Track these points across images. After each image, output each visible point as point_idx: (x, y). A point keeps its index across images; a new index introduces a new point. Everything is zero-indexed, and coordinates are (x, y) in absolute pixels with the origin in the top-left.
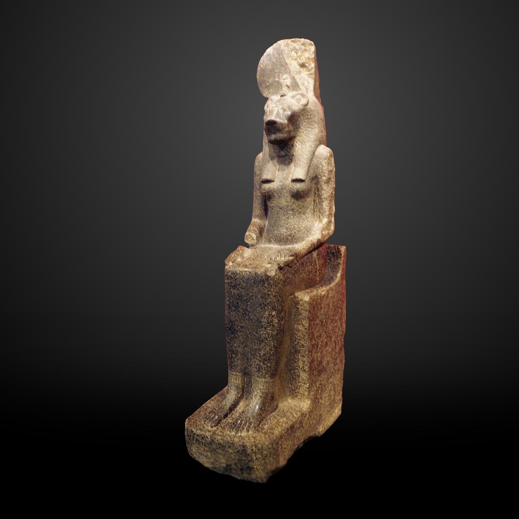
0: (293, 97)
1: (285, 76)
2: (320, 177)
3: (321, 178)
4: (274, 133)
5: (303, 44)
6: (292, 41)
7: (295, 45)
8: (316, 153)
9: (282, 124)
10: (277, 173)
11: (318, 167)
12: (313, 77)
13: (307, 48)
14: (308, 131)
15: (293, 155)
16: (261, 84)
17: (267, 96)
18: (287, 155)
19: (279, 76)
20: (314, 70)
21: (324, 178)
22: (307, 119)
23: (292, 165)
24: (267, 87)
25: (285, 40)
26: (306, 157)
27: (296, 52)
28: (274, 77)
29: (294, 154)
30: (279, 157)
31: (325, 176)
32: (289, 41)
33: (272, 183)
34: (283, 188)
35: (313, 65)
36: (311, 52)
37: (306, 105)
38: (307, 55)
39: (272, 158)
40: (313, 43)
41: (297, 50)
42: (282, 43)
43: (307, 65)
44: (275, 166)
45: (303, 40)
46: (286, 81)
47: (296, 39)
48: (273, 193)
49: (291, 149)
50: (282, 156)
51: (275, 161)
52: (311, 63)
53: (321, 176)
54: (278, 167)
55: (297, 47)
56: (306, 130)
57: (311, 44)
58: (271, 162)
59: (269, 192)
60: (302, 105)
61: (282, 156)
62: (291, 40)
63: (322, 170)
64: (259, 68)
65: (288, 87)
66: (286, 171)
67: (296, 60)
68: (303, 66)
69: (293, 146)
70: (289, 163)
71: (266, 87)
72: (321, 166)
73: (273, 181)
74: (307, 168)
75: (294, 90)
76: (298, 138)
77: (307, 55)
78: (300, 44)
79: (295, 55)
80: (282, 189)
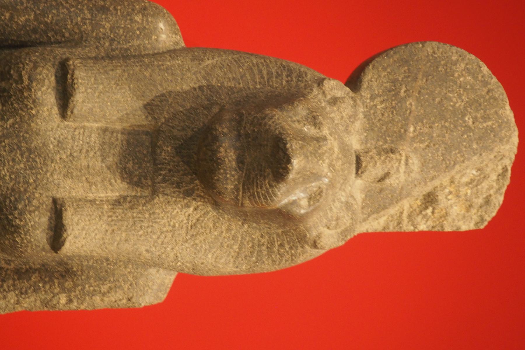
0: (348, 206)
1: (415, 163)
2: (68, 284)
3: (63, 290)
4: (240, 161)
5: (487, 201)
6: (505, 169)
7: (494, 177)
8: (153, 271)
9: (269, 196)
10: (96, 125)
11: (103, 280)
12: (391, 229)
13: (474, 211)
14: (230, 246)
15: (154, 192)
16: (404, 62)
17: (365, 85)
18: (157, 171)
19: (418, 137)
20: (411, 229)
21: (63, 300)
22: (271, 243)
23: (119, 188)
24: (392, 92)
25: (516, 151)
26: (143, 249)
27: (472, 181)
28: (419, 119)
29: (159, 199)
30: (155, 135)
31: (70, 301)
32: (508, 163)
33: (55, 110)
34: (37, 158)
35: (423, 227)
36: (460, 223)
37: (315, 245)
38: (457, 210)
39: (150, 108)
40: (482, 227)
41: (479, 183)
42: (509, 146)
43: (429, 211)
44: (121, 120)
45: (499, 200)
46: (402, 168)
47: (507, 182)
48: (15, 113)
49: (178, 185)
50: (154, 145)
51: (141, 119)
52: (430, 223)
53: (70, 291)
54: (118, 126)
55: (485, 185)
56: (234, 237)
57: (482, 220)
58: (141, 103)
59: (21, 100)
60: (319, 236)
61: (154, 145)
62: (509, 169)
63: (93, 294)
64: (455, 52)
65: (382, 179)
66: (99, 164)
67: (452, 182)
68: (430, 199)
69: (188, 194)
70: (127, 175)
71: (394, 82)
72: (104, 288)
73: (63, 115)
74: (104, 255)
75: (369, 195)
76: (213, 213)
77: (457, 210)
78: (492, 192)
79: (465, 180)
80: (30, 151)
